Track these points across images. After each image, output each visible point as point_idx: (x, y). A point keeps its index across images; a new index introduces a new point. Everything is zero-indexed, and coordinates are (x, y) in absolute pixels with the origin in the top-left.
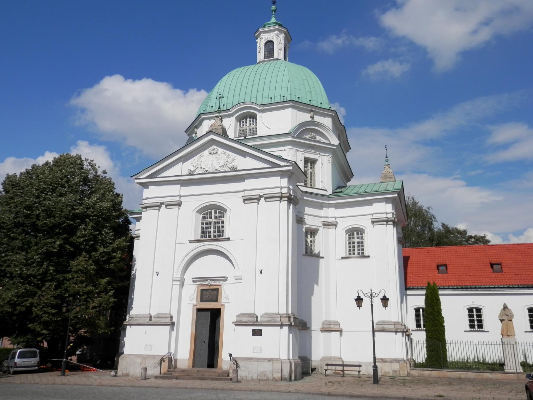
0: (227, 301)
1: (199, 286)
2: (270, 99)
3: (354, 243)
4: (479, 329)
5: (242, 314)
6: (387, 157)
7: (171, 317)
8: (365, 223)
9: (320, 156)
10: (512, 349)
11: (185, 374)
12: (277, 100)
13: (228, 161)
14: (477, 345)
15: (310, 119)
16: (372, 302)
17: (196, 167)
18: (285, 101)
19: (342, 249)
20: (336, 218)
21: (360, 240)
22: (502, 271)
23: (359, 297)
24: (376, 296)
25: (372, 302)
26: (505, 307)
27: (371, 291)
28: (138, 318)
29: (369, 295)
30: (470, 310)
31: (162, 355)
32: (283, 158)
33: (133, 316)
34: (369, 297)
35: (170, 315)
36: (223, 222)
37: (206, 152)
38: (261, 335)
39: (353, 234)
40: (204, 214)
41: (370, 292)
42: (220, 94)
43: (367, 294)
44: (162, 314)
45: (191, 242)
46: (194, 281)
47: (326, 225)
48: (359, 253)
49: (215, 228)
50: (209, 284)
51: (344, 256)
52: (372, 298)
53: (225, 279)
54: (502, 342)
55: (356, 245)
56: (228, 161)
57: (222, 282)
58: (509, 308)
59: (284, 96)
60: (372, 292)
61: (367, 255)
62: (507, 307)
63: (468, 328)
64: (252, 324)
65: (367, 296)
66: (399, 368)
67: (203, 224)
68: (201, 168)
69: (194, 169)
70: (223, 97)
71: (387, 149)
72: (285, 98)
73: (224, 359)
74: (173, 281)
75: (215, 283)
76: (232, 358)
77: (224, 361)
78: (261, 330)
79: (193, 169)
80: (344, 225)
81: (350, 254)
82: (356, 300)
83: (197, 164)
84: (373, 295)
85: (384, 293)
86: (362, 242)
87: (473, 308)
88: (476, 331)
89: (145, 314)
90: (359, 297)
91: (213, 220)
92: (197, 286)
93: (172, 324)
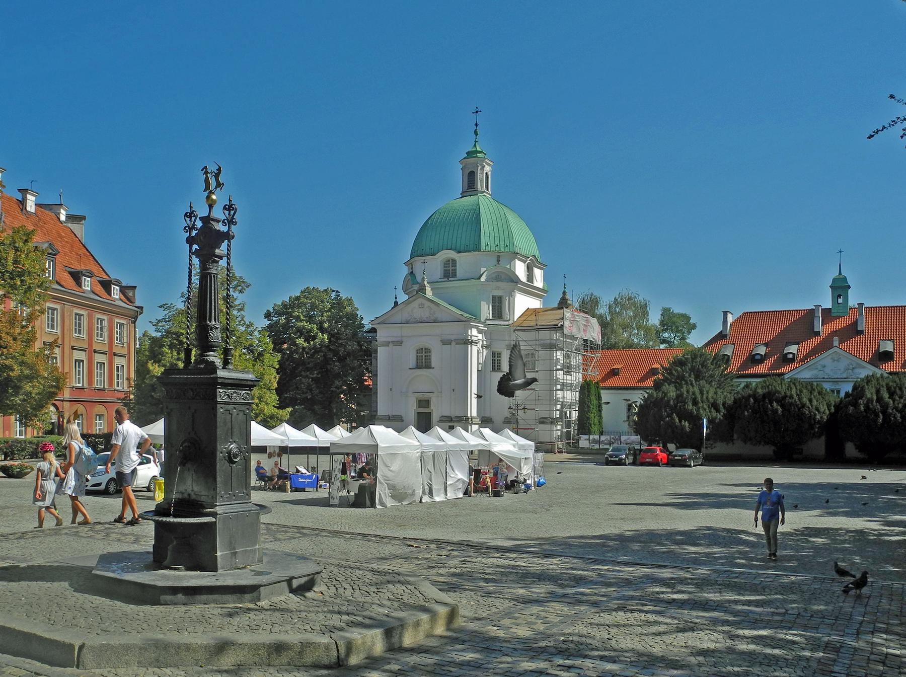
5: (443, 416)
36: (430, 356)
57: (430, 395)
67: (417, 356)
91: (424, 354)
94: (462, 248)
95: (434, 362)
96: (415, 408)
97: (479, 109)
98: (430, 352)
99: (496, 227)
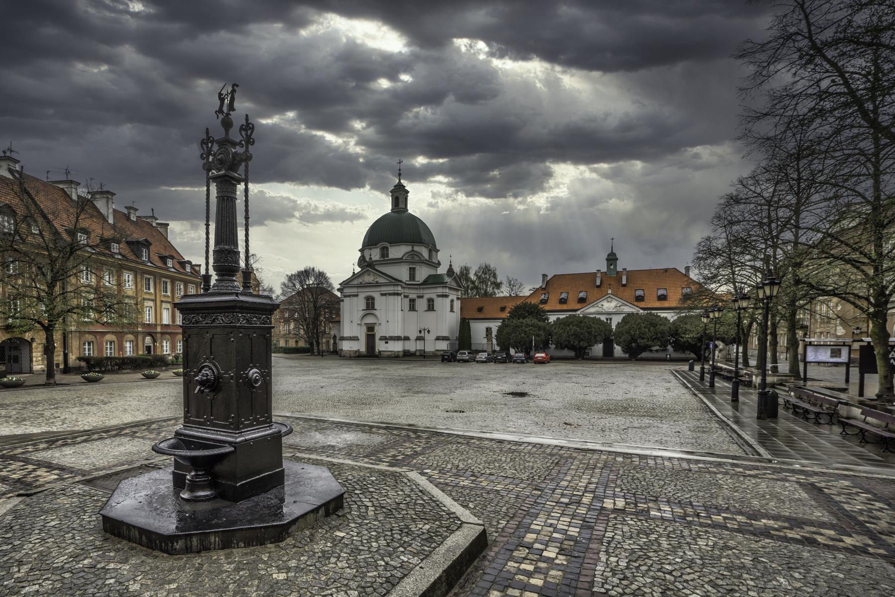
8: (434, 296)
19: (425, 307)
30: (487, 329)
47: (419, 297)
80: (426, 297)
95: (377, 305)
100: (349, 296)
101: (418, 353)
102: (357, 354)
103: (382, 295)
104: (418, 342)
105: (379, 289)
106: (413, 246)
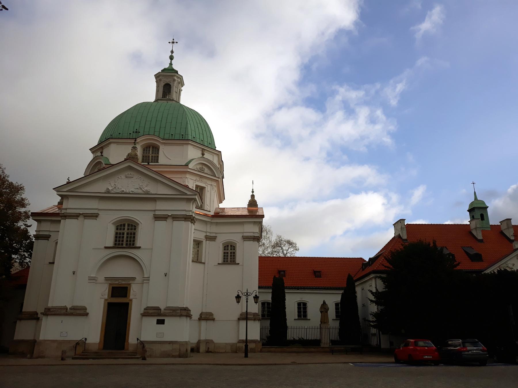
0: (135, 297)
1: (110, 284)
2: (171, 135)
3: (228, 253)
4: (304, 318)
6: (253, 190)
7: (86, 309)
8: (236, 239)
9: (208, 185)
10: (328, 331)
11: (97, 355)
12: (177, 137)
13: (142, 185)
14: (307, 329)
15: (202, 156)
16: (247, 299)
17: (114, 187)
18: (183, 139)
20: (216, 233)
21: (233, 251)
22: (321, 277)
23: (238, 295)
24: (250, 295)
25: (247, 299)
26: (324, 303)
27: (247, 291)
28: (55, 310)
29: (246, 294)
30: (299, 304)
31: (78, 340)
32: (190, 188)
33: (50, 308)
34: (246, 295)
35: (85, 307)
36: (134, 234)
37: (123, 177)
38: (164, 323)
39: (228, 246)
40: (118, 226)
41: (246, 292)
42: (137, 130)
43: (244, 293)
44: (77, 306)
45: (106, 248)
46: (106, 280)
47: (208, 238)
48: (231, 261)
49: (127, 237)
50: (120, 283)
51: (220, 262)
52: (247, 296)
53: (134, 279)
54: (321, 327)
55: (229, 255)
56: (142, 185)
58: (326, 303)
59: (182, 135)
60: (248, 292)
61: (237, 263)
62: (325, 303)
63: (297, 318)
64: (157, 315)
65: (244, 294)
66: (255, 346)
67: (117, 233)
68: (118, 188)
69: (112, 188)
70: (139, 132)
71: (253, 184)
72: (184, 136)
73: (130, 342)
74: (89, 279)
75: (125, 283)
76: (139, 341)
77: (130, 344)
78: (164, 320)
79: (110, 188)
80: (222, 239)
81: (224, 261)
82: (236, 297)
83: (115, 184)
84: (248, 294)
85: (256, 293)
86: (234, 253)
87: (301, 302)
88: (302, 319)
89: (62, 307)
90: (238, 295)
92: (108, 284)
93: (87, 314)
94: (167, 137)
96: (106, 297)
97: (175, 41)
98: (135, 229)
99: (199, 125)
100: (76, 216)
101: (202, 348)
102: (80, 350)
103: (157, 218)
104: (203, 323)
105: (149, 206)
106: (203, 150)
